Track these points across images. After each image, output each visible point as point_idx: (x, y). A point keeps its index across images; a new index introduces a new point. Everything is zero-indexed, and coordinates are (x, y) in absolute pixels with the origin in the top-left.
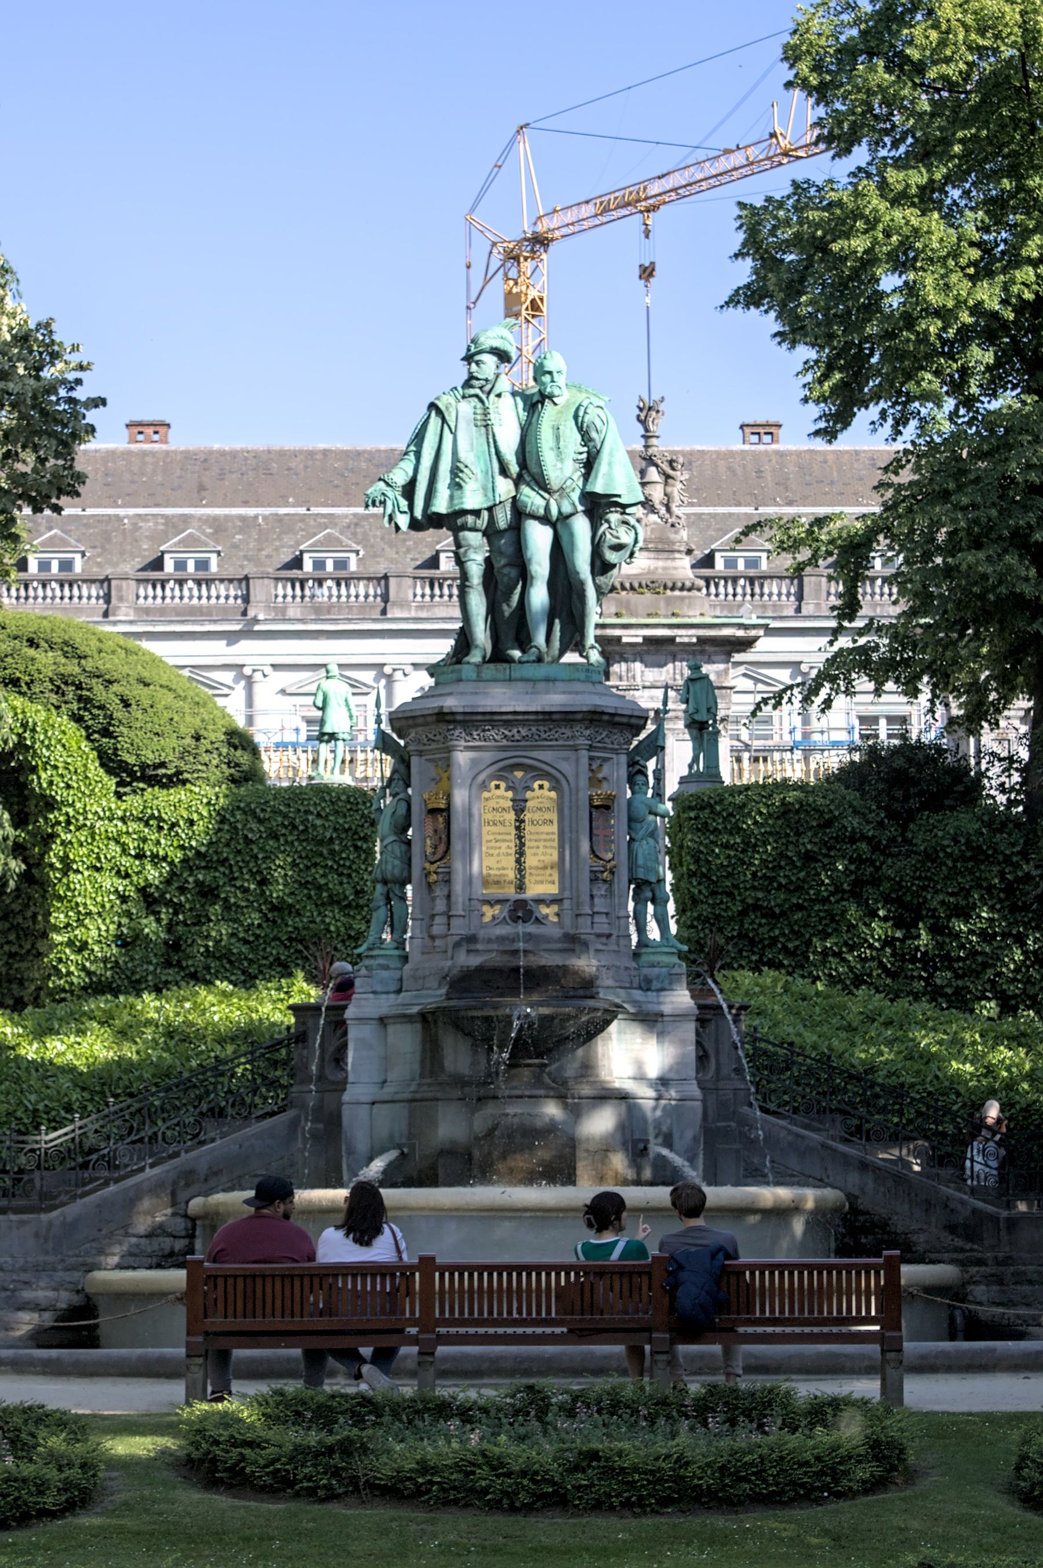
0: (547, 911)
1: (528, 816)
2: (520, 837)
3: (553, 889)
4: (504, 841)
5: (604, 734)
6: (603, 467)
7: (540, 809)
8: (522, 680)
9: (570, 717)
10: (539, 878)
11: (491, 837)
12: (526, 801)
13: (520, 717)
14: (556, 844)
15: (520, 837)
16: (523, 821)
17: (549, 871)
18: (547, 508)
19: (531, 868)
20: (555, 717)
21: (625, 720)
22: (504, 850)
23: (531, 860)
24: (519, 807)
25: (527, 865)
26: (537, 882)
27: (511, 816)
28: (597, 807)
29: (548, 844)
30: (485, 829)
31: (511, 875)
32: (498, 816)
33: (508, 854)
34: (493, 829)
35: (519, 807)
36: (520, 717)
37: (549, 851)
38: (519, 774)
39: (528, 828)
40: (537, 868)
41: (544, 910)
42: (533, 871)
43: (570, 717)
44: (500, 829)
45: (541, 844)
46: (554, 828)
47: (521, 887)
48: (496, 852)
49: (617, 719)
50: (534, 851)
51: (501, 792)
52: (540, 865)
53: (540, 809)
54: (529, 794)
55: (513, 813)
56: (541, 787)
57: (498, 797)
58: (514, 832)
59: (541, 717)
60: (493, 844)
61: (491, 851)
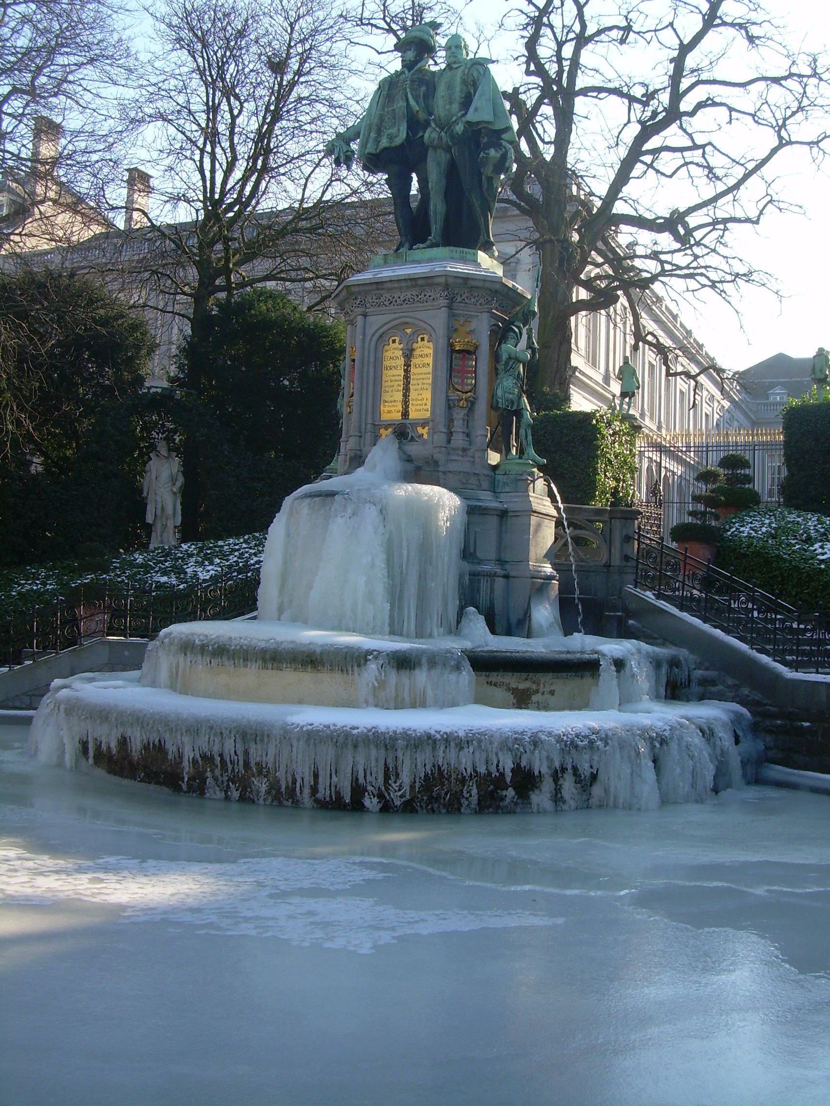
0: (424, 431)
1: (414, 361)
2: (407, 377)
3: (428, 415)
4: (396, 381)
5: (466, 294)
6: (476, 102)
7: (421, 356)
8: (414, 262)
9: (430, 281)
10: (419, 407)
11: (388, 379)
12: (412, 350)
13: (396, 285)
14: (430, 381)
15: (407, 377)
16: (410, 365)
17: (425, 401)
18: (440, 138)
19: (413, 400)
20: (420, 282)
21: (480, 284)
22: (396, 387)
23: (413, 395)
24: (408, 355)
25: (410, 398)
26: (416, 410)
27: (402, 361)
28: (459, 352)
29: (424, 381)
30: (385, 372)
31: (400, 407)
32: (393, 363)
33: (398, 391)
34: (391, 372)
35: (408, 355)
36: (396, 285)
37: (425, 386)
38: (409, 331)
39: (413, 370)
40: (417, 400)
41: (420, 430)
42: (414, 402)
43: (430, 281)
44: (394, 372)
45: (420, 382)
46: (430, 369)
47: (405, 414)
48: (390, 389)
49: (470, 283)
50: (417, 387)
51: (397, 345)
52: (420, 397)
53: (421, 356)
54: (415, 346)
55: (403, 359)
56: (423, 339)
57: (394, 349)
58: (403, 374)
59: (409, 283)
60: (389, 383)
61: (387, 389)
